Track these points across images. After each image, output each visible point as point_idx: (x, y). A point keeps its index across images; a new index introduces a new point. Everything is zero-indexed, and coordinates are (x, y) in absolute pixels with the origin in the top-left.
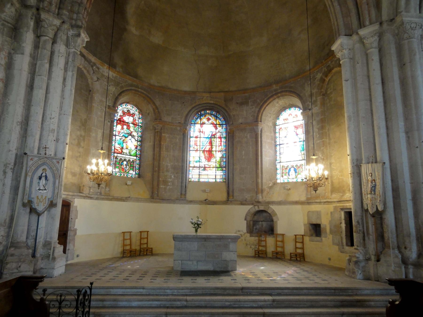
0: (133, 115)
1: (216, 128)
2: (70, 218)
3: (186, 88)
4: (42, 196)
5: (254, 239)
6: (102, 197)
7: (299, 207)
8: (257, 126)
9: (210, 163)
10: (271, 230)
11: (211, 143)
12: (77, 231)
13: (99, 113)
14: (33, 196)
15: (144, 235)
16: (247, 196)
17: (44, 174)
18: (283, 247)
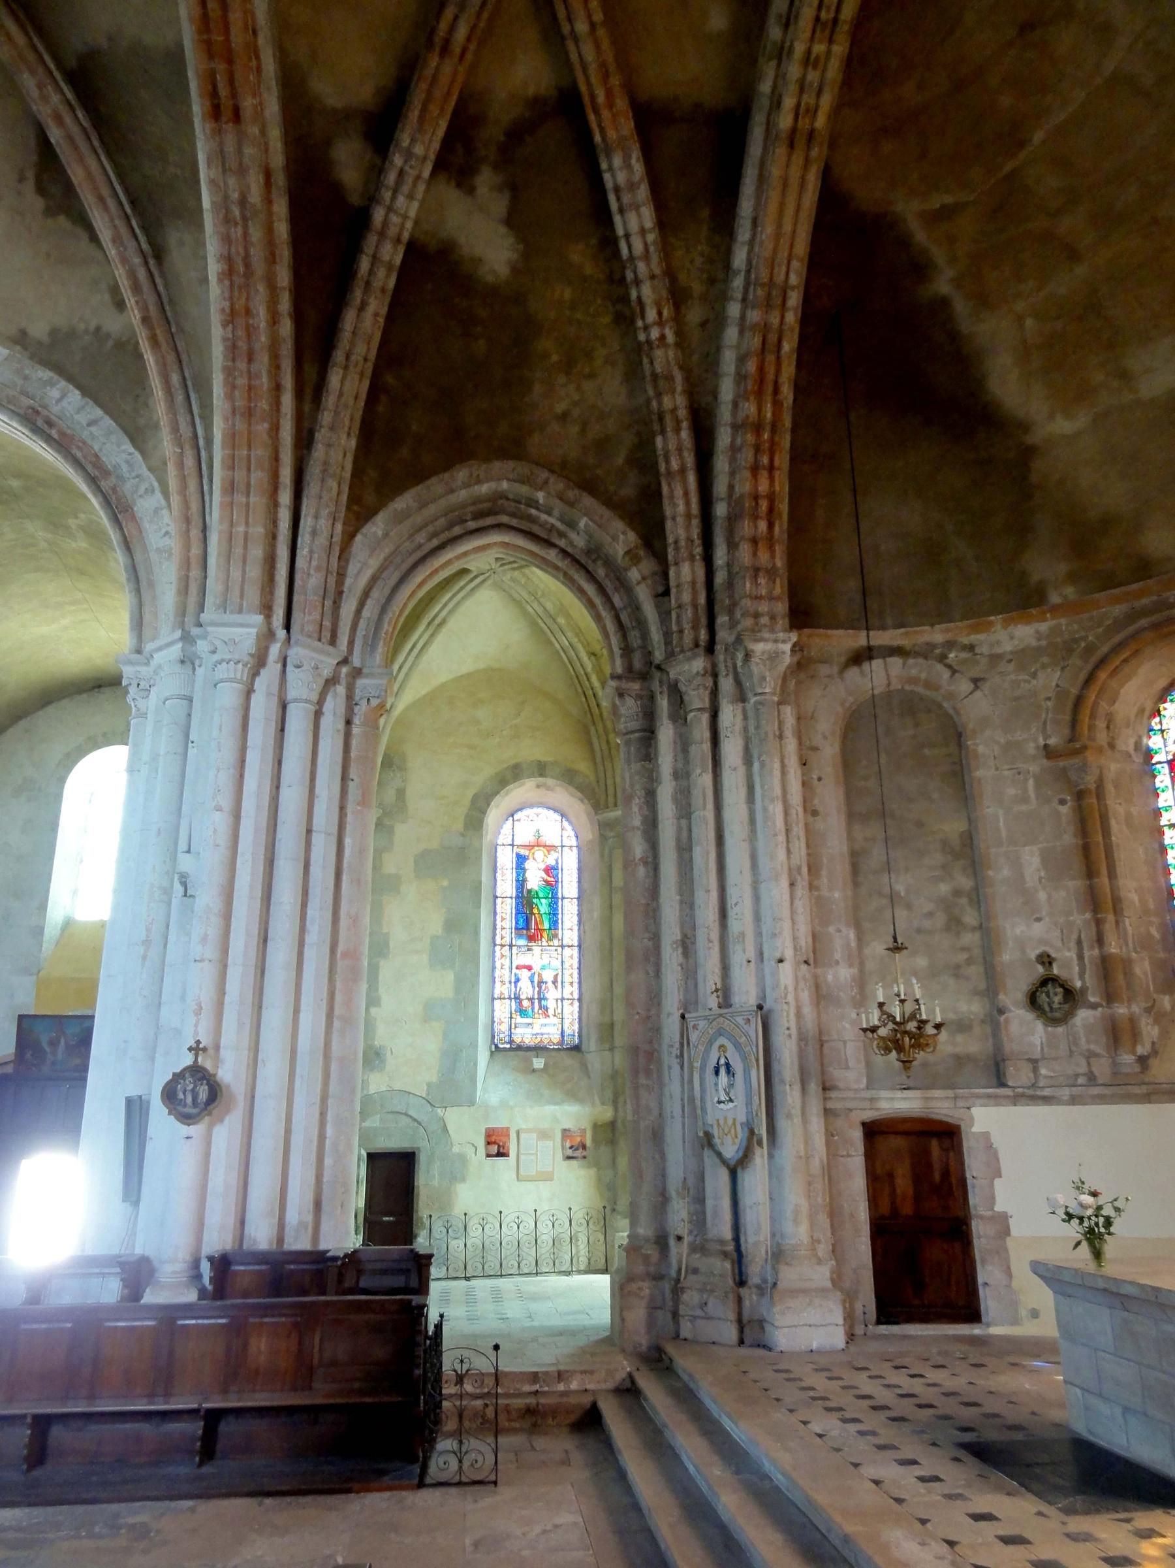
2: (968, 1176)
4: (725, 1119)
6: (1095, 1091)
12: (1011, 1221)
13: (1011, 791)
14: (710, 1120)
17: (722, 1061)
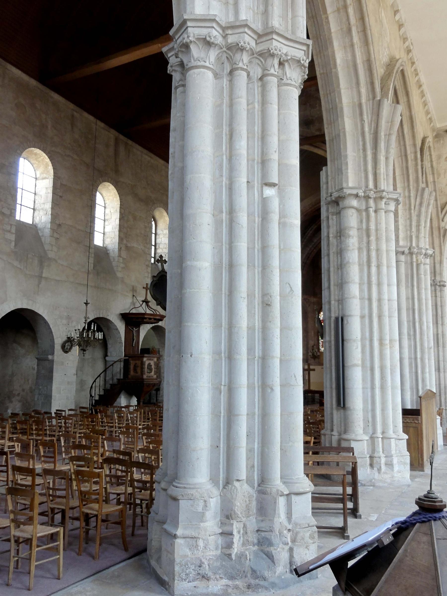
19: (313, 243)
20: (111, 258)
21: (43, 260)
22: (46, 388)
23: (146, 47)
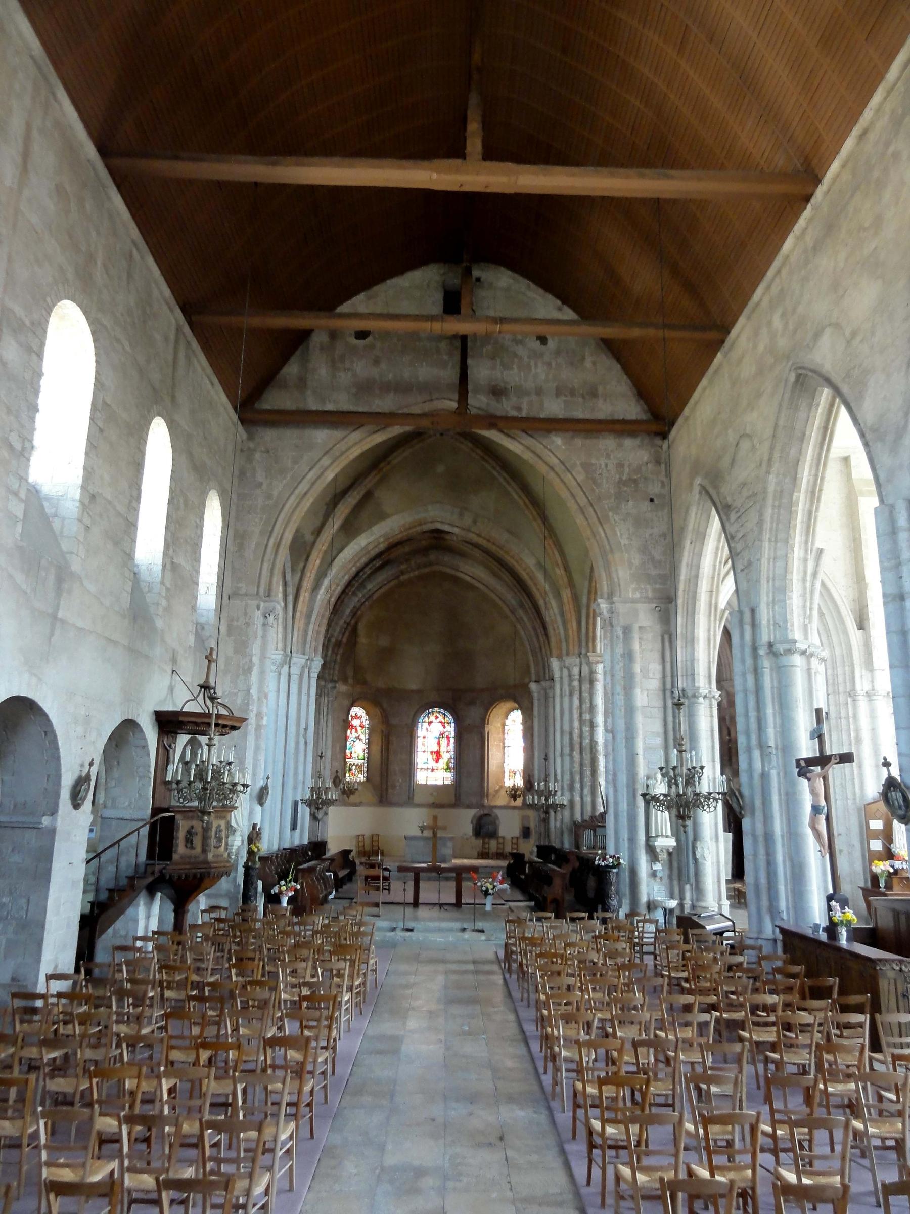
0: (361, 717)
1: (444, 728)
3: (414, 687)
5: (479, 842)
7: (516, 812)
8: (484, 728)
9: (437, 765)
10: (493, 834)
11: (439, 743)
15: (375, 838)
16: (474, 800)
18: (503, 849)
19: (365, 591)
20: (143, 585)
21: (64, 577)
22: (23, 901)
23: (400, 168)
